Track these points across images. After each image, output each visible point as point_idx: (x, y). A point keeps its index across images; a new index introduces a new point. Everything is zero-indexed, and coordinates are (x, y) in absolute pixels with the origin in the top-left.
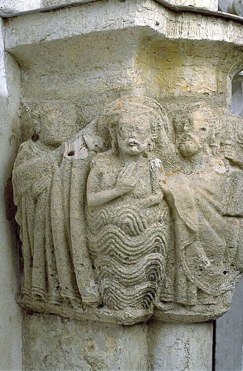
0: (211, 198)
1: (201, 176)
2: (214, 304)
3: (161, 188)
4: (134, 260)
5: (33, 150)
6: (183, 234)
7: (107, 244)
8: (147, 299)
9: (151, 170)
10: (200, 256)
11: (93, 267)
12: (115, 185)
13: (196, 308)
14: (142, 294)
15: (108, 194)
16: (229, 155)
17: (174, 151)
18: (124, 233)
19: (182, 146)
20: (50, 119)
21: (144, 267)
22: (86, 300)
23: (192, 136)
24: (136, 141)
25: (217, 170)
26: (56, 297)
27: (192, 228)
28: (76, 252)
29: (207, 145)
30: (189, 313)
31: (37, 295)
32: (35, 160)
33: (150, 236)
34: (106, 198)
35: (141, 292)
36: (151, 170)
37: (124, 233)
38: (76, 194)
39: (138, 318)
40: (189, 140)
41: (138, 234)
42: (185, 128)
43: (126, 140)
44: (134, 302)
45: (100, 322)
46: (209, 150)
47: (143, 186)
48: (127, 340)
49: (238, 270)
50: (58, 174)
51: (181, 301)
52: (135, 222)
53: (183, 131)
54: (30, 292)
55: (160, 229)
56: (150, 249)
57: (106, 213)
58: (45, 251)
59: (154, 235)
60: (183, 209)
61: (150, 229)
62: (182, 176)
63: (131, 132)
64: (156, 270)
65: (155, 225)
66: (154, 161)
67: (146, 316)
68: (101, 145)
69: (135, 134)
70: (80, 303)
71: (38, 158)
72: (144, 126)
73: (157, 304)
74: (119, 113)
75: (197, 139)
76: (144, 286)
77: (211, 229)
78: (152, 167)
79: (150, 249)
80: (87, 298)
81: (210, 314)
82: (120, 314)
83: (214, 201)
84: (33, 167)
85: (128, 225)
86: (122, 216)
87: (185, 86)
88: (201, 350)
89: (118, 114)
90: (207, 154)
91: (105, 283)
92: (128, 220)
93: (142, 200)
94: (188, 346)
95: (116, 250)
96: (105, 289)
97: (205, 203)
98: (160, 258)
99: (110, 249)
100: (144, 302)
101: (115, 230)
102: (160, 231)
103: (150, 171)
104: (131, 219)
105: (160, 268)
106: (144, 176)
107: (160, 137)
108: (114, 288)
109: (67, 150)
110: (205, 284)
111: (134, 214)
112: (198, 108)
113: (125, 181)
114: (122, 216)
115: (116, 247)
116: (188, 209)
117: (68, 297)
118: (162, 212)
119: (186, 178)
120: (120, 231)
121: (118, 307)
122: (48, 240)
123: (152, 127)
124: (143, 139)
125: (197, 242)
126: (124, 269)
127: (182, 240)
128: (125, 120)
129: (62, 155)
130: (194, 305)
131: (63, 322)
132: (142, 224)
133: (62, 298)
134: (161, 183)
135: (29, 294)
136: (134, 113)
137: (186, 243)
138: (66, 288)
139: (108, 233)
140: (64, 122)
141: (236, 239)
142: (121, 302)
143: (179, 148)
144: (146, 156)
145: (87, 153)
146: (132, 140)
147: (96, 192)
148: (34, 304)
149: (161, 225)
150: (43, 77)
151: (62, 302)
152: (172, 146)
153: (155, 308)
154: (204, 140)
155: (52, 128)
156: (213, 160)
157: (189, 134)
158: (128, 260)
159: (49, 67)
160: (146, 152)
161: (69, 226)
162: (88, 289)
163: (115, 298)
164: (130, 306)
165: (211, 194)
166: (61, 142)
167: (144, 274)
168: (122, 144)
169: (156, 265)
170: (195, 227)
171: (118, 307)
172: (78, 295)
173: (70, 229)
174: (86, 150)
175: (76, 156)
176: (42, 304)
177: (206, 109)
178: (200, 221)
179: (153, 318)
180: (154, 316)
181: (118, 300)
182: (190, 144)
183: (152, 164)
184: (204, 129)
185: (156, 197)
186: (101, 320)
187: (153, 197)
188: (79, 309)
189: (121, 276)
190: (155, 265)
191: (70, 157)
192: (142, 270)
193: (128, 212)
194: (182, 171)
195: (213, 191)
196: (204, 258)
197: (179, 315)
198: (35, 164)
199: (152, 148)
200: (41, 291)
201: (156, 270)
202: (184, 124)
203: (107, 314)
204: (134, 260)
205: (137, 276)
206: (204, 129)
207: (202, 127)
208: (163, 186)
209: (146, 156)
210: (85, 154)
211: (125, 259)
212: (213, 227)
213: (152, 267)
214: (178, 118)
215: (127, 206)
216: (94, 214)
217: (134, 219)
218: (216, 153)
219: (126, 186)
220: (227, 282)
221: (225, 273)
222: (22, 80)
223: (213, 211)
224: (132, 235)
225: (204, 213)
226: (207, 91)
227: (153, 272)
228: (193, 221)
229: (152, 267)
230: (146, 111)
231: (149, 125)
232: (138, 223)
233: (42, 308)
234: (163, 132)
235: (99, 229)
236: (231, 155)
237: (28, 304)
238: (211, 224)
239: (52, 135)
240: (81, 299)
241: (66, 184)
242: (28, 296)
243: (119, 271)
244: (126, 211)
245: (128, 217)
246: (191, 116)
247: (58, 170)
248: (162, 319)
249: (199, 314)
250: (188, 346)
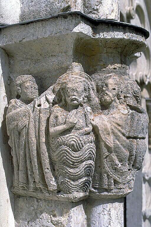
0: (120, 128)
1: (114, 116)
2: (124, 188)
3: (91, 124)
4: (78, 165)
5: (18, 104)
6: (105, 150)
7: (62, 157)
8: (85, 187)
10: (115, 161)
11: (54, 170)
12: (65, 123)
13: (113, 191)
14: (83, 184)
15: (61, 128)
16: (129, 103)
17: (98, 102)
18: (71, 150)
19: (102, 99)
20: (26, 86)
21: (83, 169)
22: (51, 188)
23: (108, 93)
24: (76, 98)
25: (122, 112)
26: (33, 187)
27: (109, 146)
28: (44, 161)
29: (116, 98)
30: (110, 194)
31: (22, 187)
32: (18, 110)
33: (86, 151)
34: (60, 130)
35: (82, 183)
37: (71, 150)
38: (43, 128)
39: (81, 198)
40: (106, 96)
41: (79, 151)
42: (104, 88)
43: (71, 97)
44: (78, 188)
45: (59, 201)
46: (117, 101)
47: (81, 123)
48: (75, 210)
49: (136, 168)
50: (32, 117)
51: (106, 187)
52: (77, 143)
53: (103, 91)
54: (18, 185)
55: (91, 146)
56: (86, 158)
57: (60, 139)
58: (26, 161)
59: (88, 150)
60: (104, 135)
61: (86, 147)
62: (103, 116)
64: (90, 170)
65: (89, 144)
66: (87, 108)
67: (85, 196)
68: (56, 100)
69: (75, 94)
70: (47, 190)
71: (21, 109)
72: (81, 88)
73: (91, 189)
75: (111, 95)
76: (84, 179)
77: (120, 146)
79: (86, 158)
80: (51, 187)
81: (121, 194)
82: (71, 196)
83: (121, 130)
84: (17, 113)
85: (73, 145)
86: (70, 140)
87: (103, 65)
88: (117, 214)
89: (65, 83)
90: (117, 103)
91: (61, 180)
92: (73, 142)
93: (81, 131)
94: (110, 213)
95: (67, 160)
96: (61, 182)
97: (117, 131)
98: (92, 163)
99: (63, 159)
100: (84, 189)
101: (66, 148)
102: (91, 148)
103: (85, 114)
104: (75, 142)
105: (92, 169)
106: (82, 117)
107: (90, 94)
108: (67, 181)
109: (37, 103)
110: (118, 177)
111: (76, 138)
112: (111, 77)
113: (71, 121)
114: (70, 140)
115: (67, 158)
116: (107, 135)
117: (40, 187)
118: (92, 137)
119: (105, 118)
120: (69, 149)
121: (69, 192)
122: (27, 155)
123: (85, 90)
124: (80, 96)
125: (113, 153)
126: (72, 170)
127: (104, 152)
128: (70, 85)
129: (34, 106)
130: (112, 189)
131: (37, 201)
132: (81, 144)
133: (37, 188)
134: (91, 121)
135: (17, 186)
136: (75, 81)
137: (107, 154)
138: (39, 182)
139: (62, 150)
140: (35, 87)
141: (135, 150)
142: (71, 189)
144: (82, 106)
145: (49, 105)
146: (74, 97)
147: (55, 126)
148: (21, 192)
149: (92, 144)
150: (21, 62)
151: (37, 190)
152: (97, 99)
153: (91, 192)
154: (114, 95)
155: (28, 91)
156: (120, 106)
157: (106, 92)
158: (74, 165)
159: (25, 56)
160: (82, 103)
161: (40, 146)
162: (51, 182)
163: (67, 187)
164: (76, 191)
165: (120, 126)
166: (33, 98)
167: (83, 173)
168: (68, 100)
169: (90, 167)
170: (111, 145)
171: (69, 192)
172: (46, 185)
173: (40, 149)
174: (48, 103)
175: (42, 107)
176: (25, 192)
177: (115, 77)
178: (114, 141)
179: (89, 197)
180: (89, 196)
181: (69, 188)
182: (107, 98)
183: (86, 110)
184: (114, 89)
185: (88, 128)
186: (60, 200)
187: (87, 129)
188: (47, 193)
189: (70, 174)
190: (89, 167)
191: (39, 108)
192: (82, 170)
193: (73, 138)
194: (103, 113)
195: (121, 124)
196: (117, 162)
197: (104, 195)
198: (19, 112)
199: (85, 101)
200: (24, 184)
201: (90, 170)
202: (103, 87)
203: (63, 196)
204: (78, 165)
205: (80, 174)
206: (114, 89)
207: (113, 88)
208: (93, 122)
209: (82, 106)
210: (47, 105)
211: (72, 165)
212: (121, 144)
213: (88, 169)
214: (100, 84)
215: (72, 134)
216: (53, 140)
217: (77, 142)
218: (122, 103)
219: (71, 123)
220: (131, 175)
221: (129, 170)
222: (9, 63)
223: (121, 135)
224: (76, 151)
225: (117, 137)
226: (115, 67)
227: (88, 172)
228: (110, 142)
229: (88, 169)
230: (81, 80)
231: (83, 88)
232: (78, 144)
233: (25, 194)
234: (92, 92)
235: (57, 148)
236: (130, 103)
237: (17, 192)
238: (120, 143)
239: (28, 95)
240: (48, 188)
241: (37, 123)
242: (17, 187)
243: (69, 171)
244: (72, 137)
245: (73, 141)
246: (106, 81)
247: (32, 115)
248: (95, 198)
249: (115, 194)
250: (110, 213)
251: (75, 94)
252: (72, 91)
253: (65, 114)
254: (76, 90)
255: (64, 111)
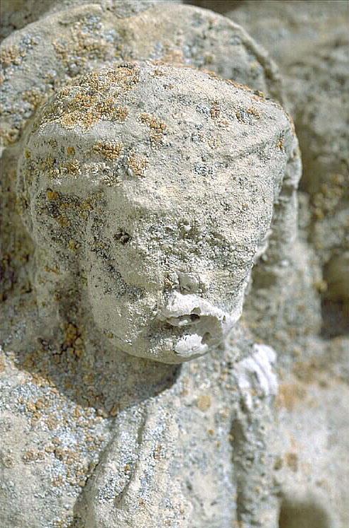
3: (280, 495)
9: (241, 416)
24: (209, 307)
36: (241, 416)
43: (151, 300)
47: (207, 505)
63: (183, 258)
74: (117, 142)
78: (249, 403)
89: (105, 152)
143: (326, 268)
146: (184, 303)
183: (244, 384)
251: (203, 271)
252: (167, 243)
253: (68, 440)
254: (217, 240)
255: (60, 406)
